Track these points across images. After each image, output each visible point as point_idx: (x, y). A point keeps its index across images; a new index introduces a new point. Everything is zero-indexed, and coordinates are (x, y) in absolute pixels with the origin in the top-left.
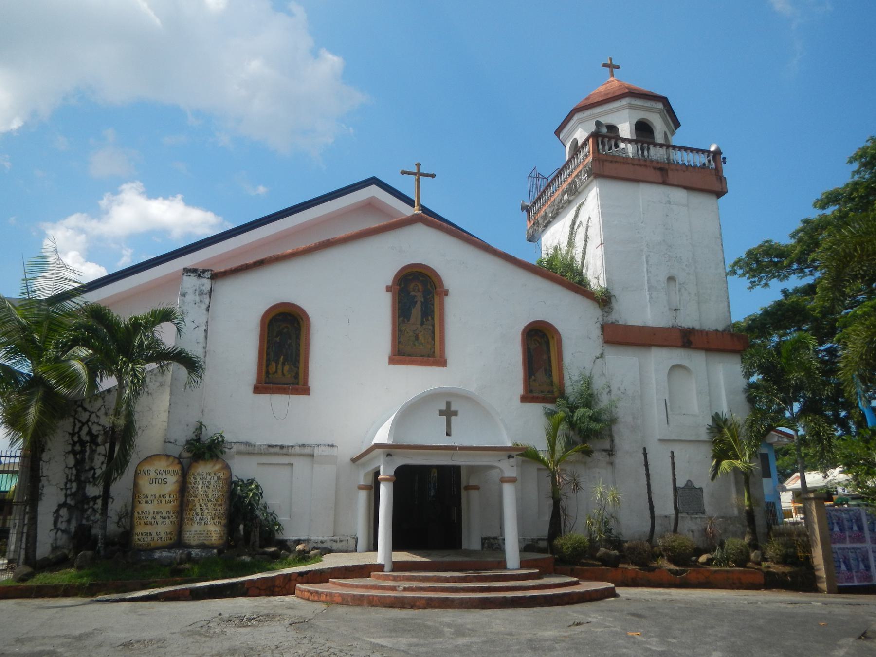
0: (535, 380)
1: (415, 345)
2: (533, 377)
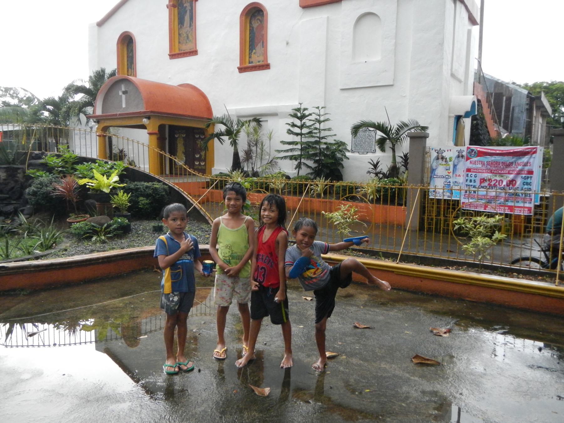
0: (255, 53)
1: (187, 42)
2: (254, 51)
